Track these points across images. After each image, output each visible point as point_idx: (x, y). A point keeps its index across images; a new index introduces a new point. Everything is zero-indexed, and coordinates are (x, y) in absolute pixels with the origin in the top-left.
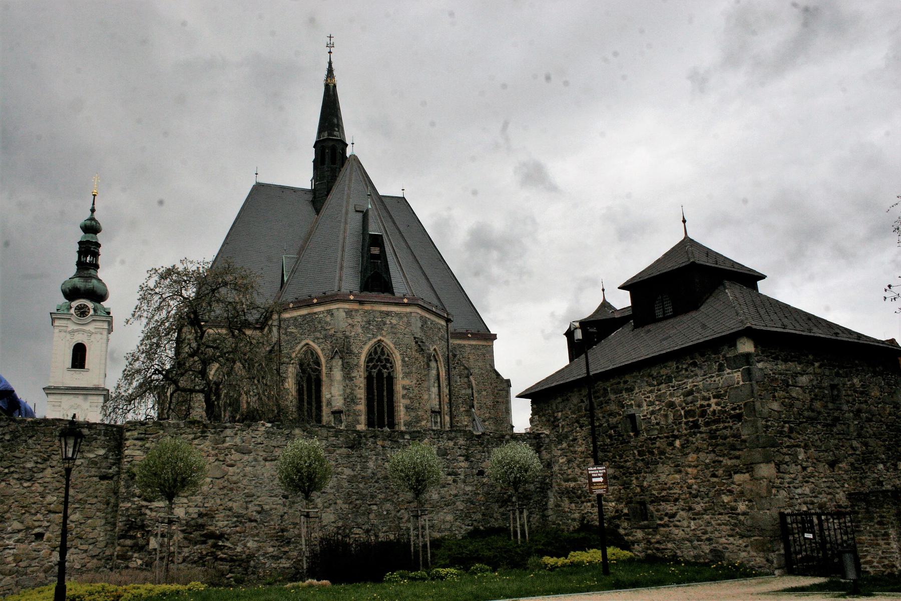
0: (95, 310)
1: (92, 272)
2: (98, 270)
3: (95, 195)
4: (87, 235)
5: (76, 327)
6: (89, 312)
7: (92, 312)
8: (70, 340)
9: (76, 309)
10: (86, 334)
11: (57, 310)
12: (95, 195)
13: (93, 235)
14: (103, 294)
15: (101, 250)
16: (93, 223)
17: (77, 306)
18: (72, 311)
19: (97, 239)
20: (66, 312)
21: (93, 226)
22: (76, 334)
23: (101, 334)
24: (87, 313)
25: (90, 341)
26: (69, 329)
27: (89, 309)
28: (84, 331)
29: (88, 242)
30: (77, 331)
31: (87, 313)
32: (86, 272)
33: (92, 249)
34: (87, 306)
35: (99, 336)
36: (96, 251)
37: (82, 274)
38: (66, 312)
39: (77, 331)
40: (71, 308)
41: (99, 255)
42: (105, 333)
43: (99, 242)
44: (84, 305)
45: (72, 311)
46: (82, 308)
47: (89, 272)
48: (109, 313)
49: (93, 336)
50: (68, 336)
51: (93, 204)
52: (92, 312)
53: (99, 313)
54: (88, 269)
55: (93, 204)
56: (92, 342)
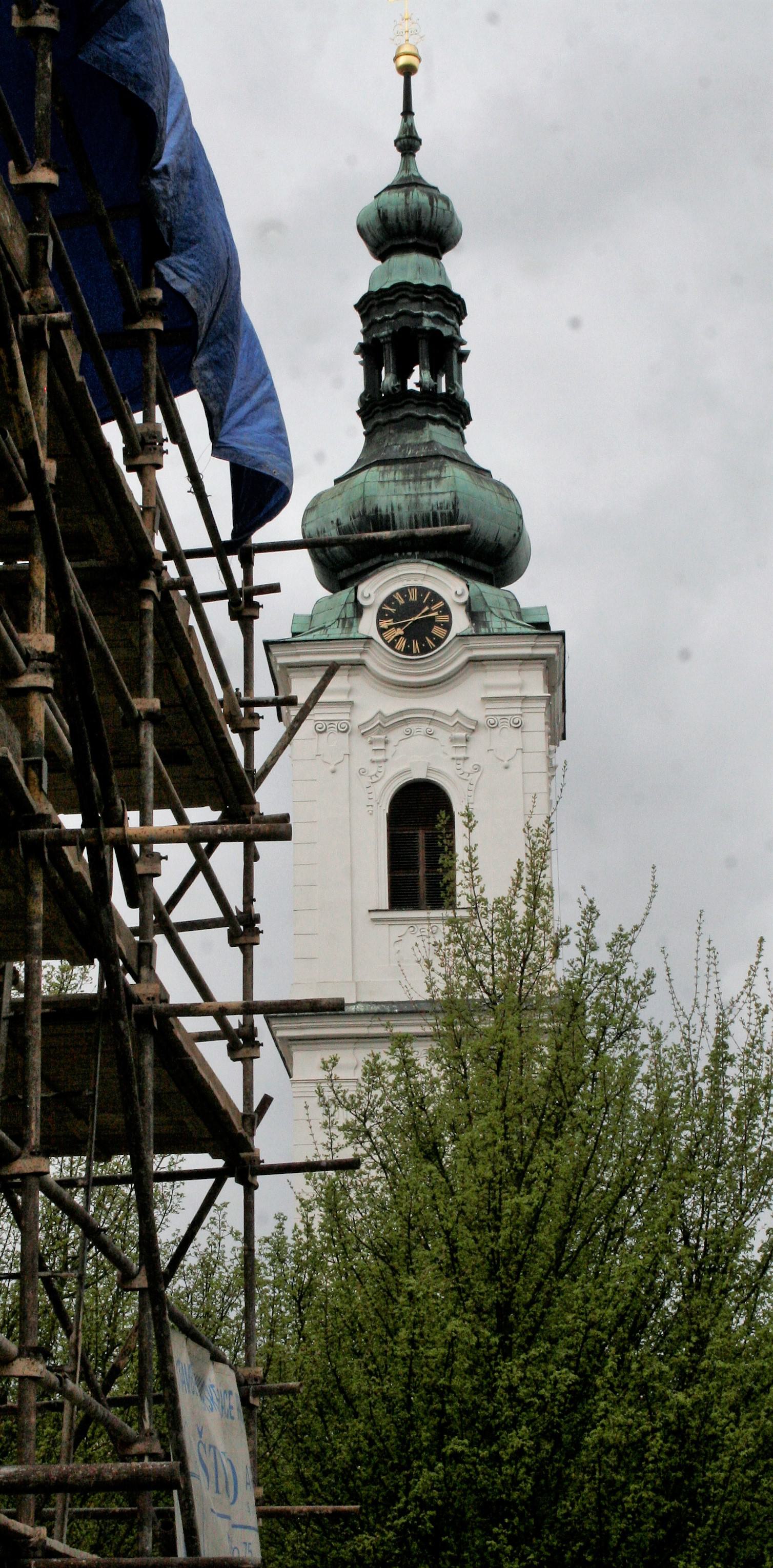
0: (474, 615)
1: (439, 435)
2: (468, 431)
3: (408, 71)
4: (396, 261)
5: (393, 704)
6: (447, 626)
7: (460, 622)
8: (373, 769)
9: (382, 615)
10: (443, 735)
11: (294, 634)
12: (408, 71)
13: (426, 260)
14: (505, 536)
15: (468, 330)
16: (418, 197)
17: (390, 600)
18: (368, 625)
19: (442, 273)
20: (336, 632)
21: (419, 211)
22: (395, 736)
23: (518, 727)
24: (437, 631)
25: (468, 767)
26: (363, 715)
27: (446, 610)
28: (432, 718)
29: (402, 290)
30: (403, 720)
31: (437, 631)
32: (410, 438)
33: (427, 324)
34: (436, 597)
35: (506, 739)
36: (446, 331)
37: (395, 451)
38: (336, 632)
39: (403, 720)
40: (359, 610)
41: (463, 356)
42: (537, 721)
43: (456, 289)
44: (422, 590)
45: (368, 625)
46: (410, 608)
47: (425, 437)
48: (544, 626)
49: (481, 739)
50: (362, 750)
51: (407, 111)
52: (460, 622)
53: (496, 624)
54: (418, 424)
55: (407, 111)
56: (477, 768)
